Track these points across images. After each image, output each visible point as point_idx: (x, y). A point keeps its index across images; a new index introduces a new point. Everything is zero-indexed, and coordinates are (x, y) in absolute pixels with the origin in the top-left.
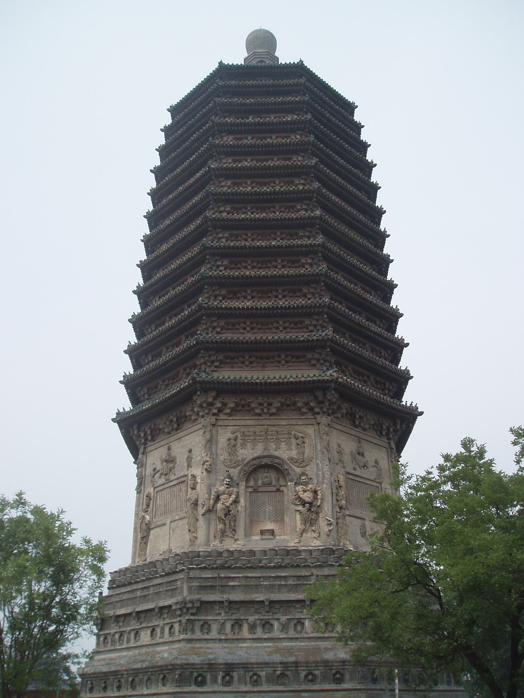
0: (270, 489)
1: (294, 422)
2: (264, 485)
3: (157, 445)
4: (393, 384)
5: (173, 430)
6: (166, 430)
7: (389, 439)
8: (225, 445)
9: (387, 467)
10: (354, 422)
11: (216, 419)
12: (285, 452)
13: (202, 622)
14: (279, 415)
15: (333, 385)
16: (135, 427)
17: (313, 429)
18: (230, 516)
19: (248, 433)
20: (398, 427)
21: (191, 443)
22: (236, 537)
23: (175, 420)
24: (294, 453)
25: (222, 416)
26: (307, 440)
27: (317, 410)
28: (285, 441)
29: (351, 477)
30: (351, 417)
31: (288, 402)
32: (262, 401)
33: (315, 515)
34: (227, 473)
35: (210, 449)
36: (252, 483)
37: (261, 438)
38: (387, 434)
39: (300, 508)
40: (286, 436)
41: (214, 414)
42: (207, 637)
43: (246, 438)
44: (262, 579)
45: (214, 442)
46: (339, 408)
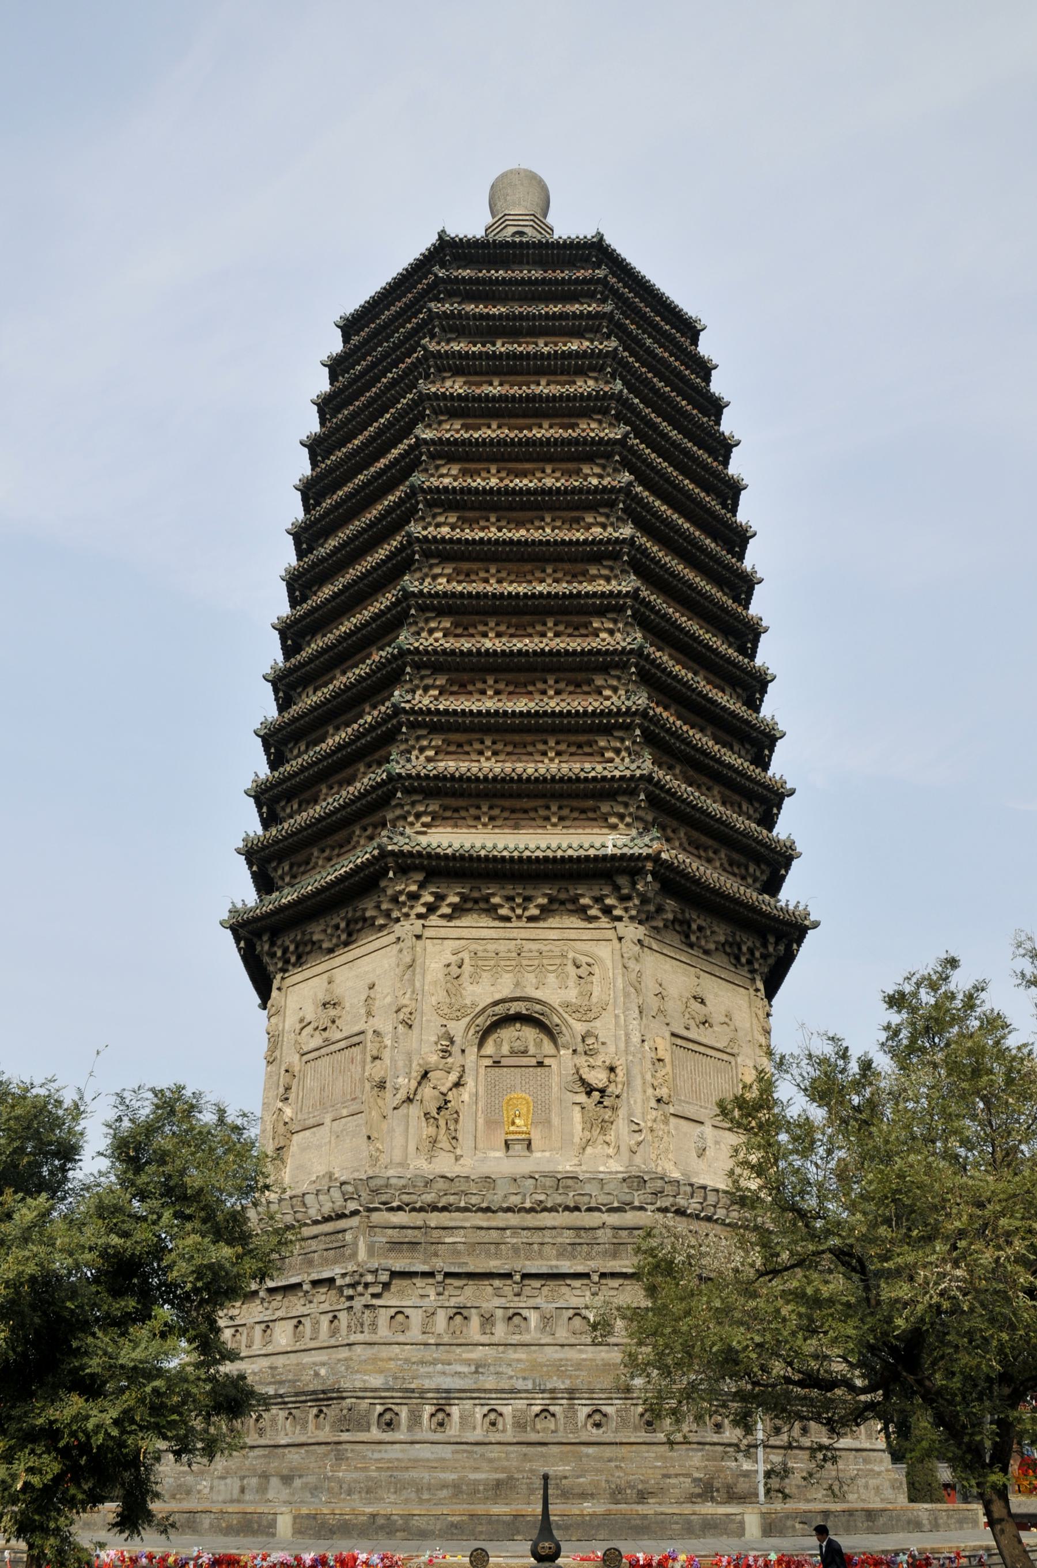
0: (525, 1061)
1: (573, 934)
2: (513, 1053)
3: (307, 974)
4: (763, 867)
5: (337, 945)
6: (325, 945)
7: (752, 971)
8: (441, 976)
9: (748, 1025)
10: (687, 937)
11: (424, 926)
12: (554, 992)
13: (393, 1311)
14: (544, 920)
15: (649, 866)
16: (265, 938)
17: (609, 949)
18: (448, 1112)
19: (485, 954)
20: (771, 949)
21: (374, 970)
22: (459, 1152)
23: (343, 925)
24: (571, 994)
25: (434, 920)
26: (596, 969)
27: (617, 912)
29: (679, 1042)
31: (563, 896)
32: (512, 893)
33: (610, 1113)
34: (444, 1029)
35: (412, 981)
36: (489, 1048)
37: (508, 963)
38: (749, 962)
39: (582, 1098)
40: (558, 961)
41: (420, 916)
42: (401, 1339)
43: (480, 963)
44: (508, 1232)
45: (418, 970)
46: (660, 910)
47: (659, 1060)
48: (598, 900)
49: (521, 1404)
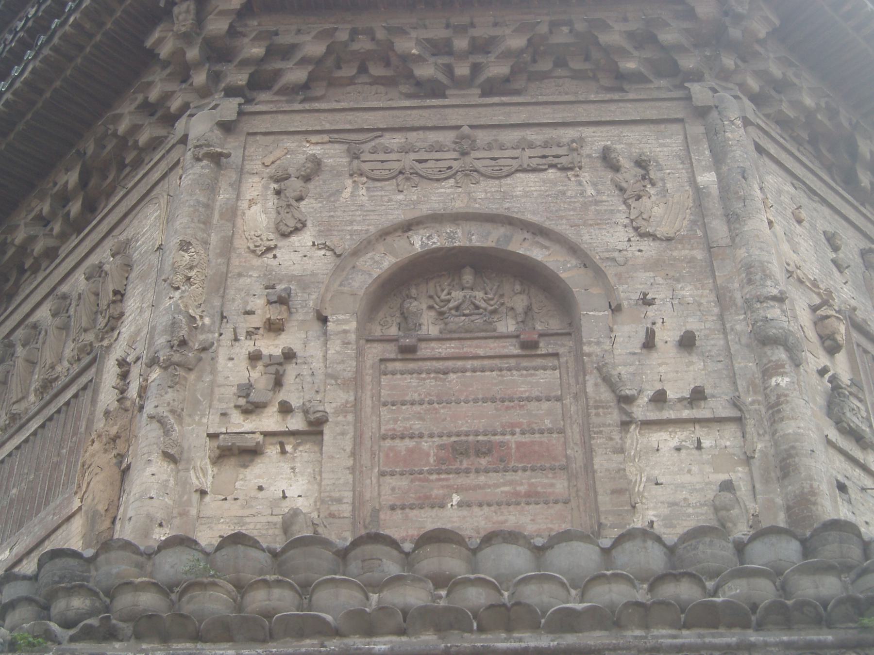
5: (63, 237)
6: (38, 248)
11: (241, 113)
25: (265, 100)
41: (231, 92)
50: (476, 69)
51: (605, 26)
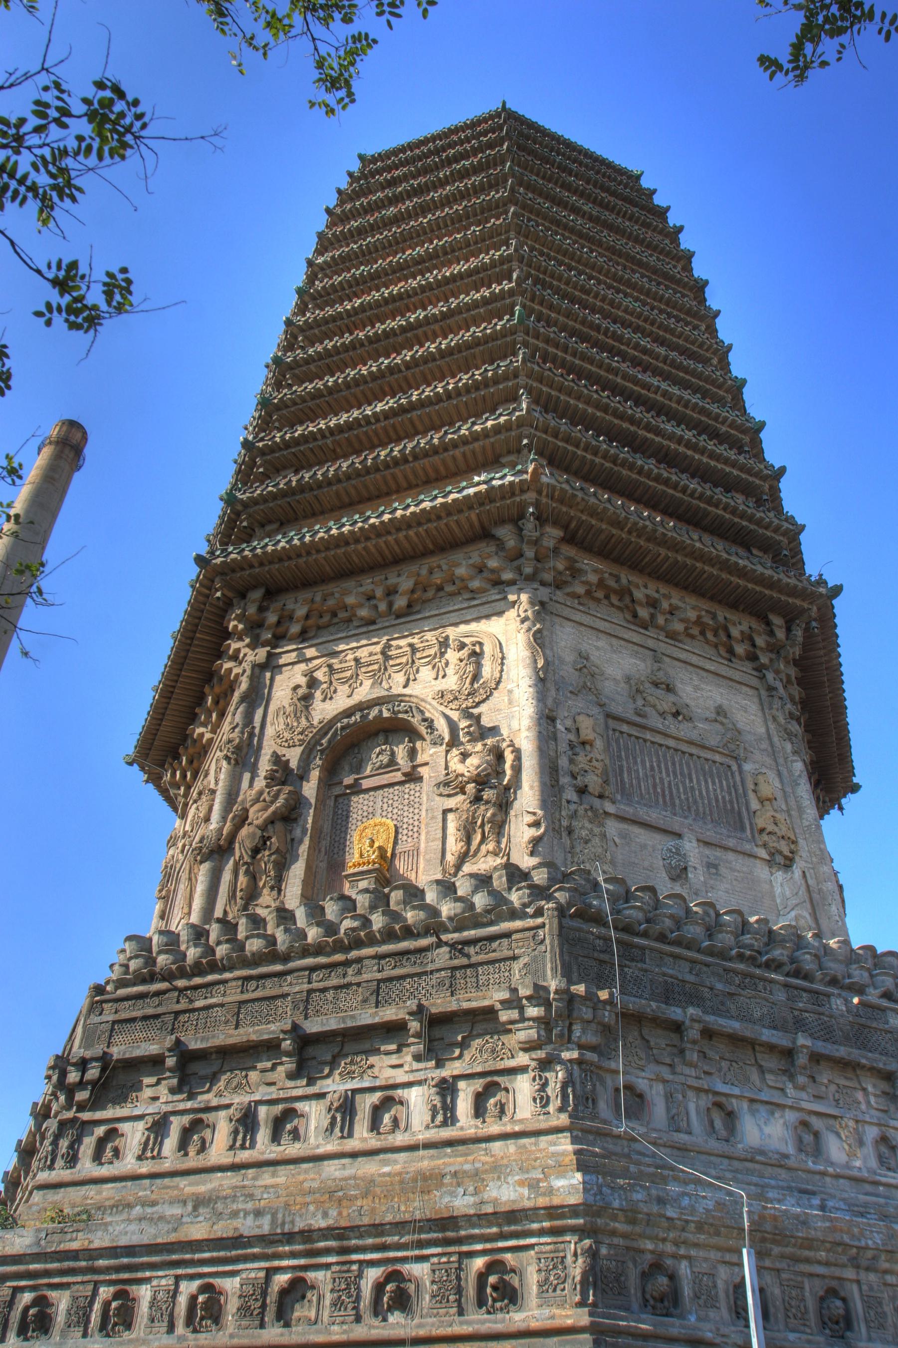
4: (755, 551)
9: (762, 730)
14: (418, 612)
27: (507, 576)
28: (429, 663)
30: (622, 598)
47: (583, 743)
48: (480, 569)
49: (254, 1271)
50: (390, 605)
51: (459, 565)
